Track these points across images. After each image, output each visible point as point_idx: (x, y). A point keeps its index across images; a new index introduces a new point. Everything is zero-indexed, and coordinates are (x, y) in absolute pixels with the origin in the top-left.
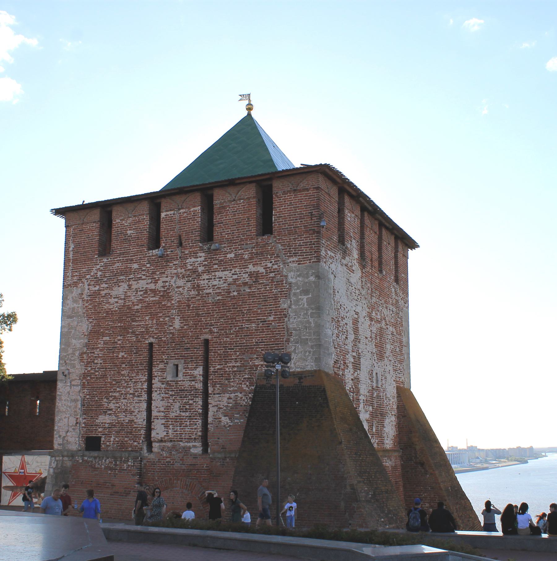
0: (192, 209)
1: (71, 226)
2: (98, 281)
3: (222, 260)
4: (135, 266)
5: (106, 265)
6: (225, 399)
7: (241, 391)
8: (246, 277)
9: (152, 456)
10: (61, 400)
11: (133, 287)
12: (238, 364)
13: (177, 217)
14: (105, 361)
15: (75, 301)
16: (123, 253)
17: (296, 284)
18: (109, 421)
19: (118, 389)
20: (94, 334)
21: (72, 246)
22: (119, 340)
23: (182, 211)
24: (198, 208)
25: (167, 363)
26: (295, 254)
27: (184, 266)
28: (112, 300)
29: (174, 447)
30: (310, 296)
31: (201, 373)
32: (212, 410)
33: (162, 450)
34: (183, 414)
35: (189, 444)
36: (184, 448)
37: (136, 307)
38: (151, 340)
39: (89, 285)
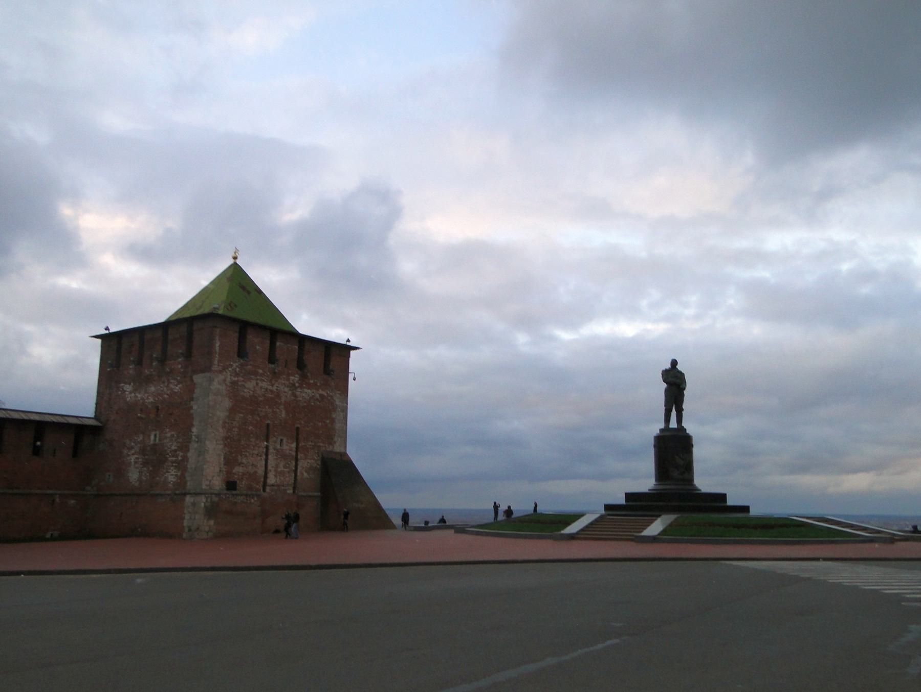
2: (237, 375)
5: (242, 365)
7: (314, 459)
15: (219, 383)
20: (232, 411)
24: (297, 347)
27: (288, 380)
38: (269, 422)
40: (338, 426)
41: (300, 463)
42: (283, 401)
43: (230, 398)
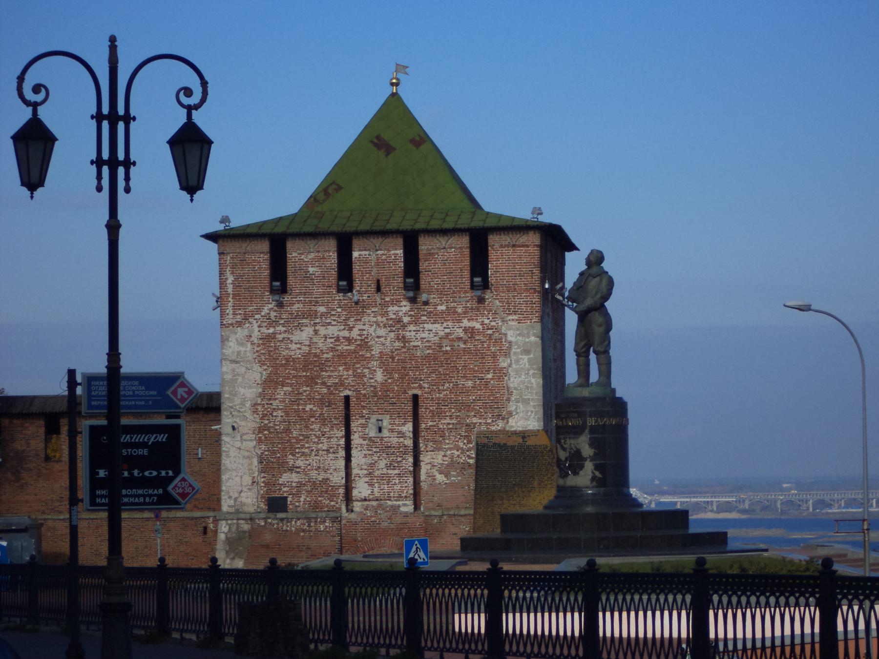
0: (392, 252)
1: (228, 254)
2: (272, 323)
3: (431, 312)
4: (322, 309)
6: (440, 457)
8: (460, 333)
9: (353, 516)
10: (228, 456)
11: (320, 333)
12: (454, 421)
13: (373, 257)
14: (287, 415)
15: (240, 344)
16: (305, 294)
17: (516, 343)
18: (296, 480)
19: (307, 445)
20: (270, 383)
21: (230, 279)
22: (305, 391)
23: (379, 252)
24: (400, 252)
25: (369, 418)
26: (515, 313)
28: (293, 347)
29: (379, 506)
30: (532, 356)
31: (411, 429)
32: (424, 469)
33: (366, 509)
34: (390, 472)
35: (398, 503)
36: (392, 506)
37: (325, 356)
39: (259, 326)
40: (514, 381)
41: (425, 458)
42: (376, 351)
43: (262, 364)
